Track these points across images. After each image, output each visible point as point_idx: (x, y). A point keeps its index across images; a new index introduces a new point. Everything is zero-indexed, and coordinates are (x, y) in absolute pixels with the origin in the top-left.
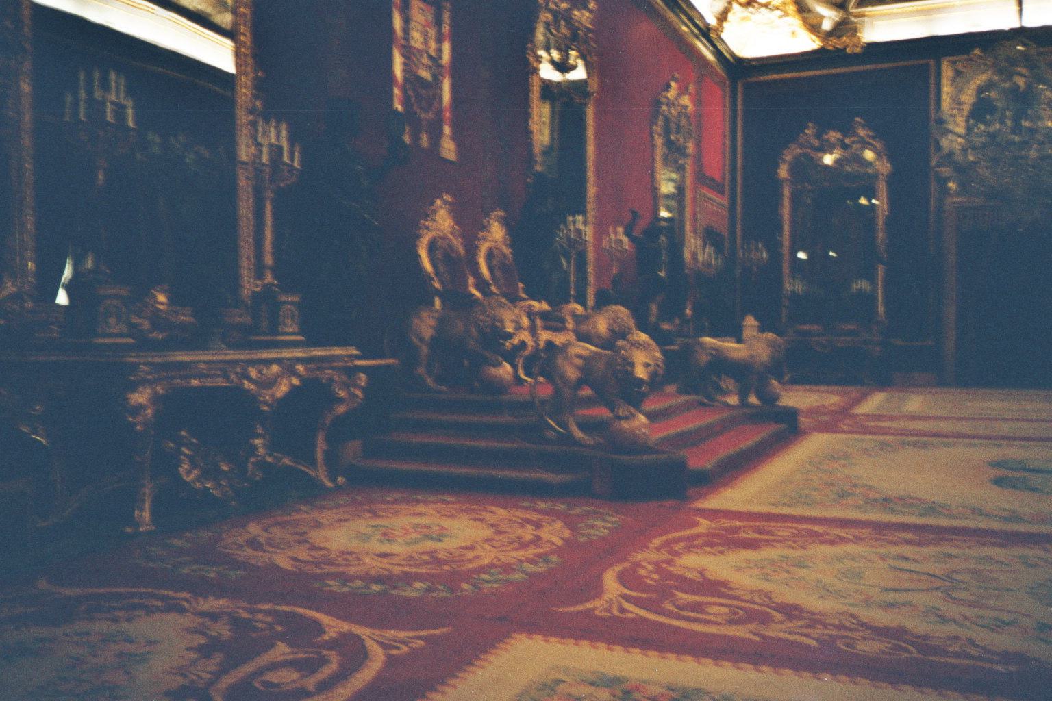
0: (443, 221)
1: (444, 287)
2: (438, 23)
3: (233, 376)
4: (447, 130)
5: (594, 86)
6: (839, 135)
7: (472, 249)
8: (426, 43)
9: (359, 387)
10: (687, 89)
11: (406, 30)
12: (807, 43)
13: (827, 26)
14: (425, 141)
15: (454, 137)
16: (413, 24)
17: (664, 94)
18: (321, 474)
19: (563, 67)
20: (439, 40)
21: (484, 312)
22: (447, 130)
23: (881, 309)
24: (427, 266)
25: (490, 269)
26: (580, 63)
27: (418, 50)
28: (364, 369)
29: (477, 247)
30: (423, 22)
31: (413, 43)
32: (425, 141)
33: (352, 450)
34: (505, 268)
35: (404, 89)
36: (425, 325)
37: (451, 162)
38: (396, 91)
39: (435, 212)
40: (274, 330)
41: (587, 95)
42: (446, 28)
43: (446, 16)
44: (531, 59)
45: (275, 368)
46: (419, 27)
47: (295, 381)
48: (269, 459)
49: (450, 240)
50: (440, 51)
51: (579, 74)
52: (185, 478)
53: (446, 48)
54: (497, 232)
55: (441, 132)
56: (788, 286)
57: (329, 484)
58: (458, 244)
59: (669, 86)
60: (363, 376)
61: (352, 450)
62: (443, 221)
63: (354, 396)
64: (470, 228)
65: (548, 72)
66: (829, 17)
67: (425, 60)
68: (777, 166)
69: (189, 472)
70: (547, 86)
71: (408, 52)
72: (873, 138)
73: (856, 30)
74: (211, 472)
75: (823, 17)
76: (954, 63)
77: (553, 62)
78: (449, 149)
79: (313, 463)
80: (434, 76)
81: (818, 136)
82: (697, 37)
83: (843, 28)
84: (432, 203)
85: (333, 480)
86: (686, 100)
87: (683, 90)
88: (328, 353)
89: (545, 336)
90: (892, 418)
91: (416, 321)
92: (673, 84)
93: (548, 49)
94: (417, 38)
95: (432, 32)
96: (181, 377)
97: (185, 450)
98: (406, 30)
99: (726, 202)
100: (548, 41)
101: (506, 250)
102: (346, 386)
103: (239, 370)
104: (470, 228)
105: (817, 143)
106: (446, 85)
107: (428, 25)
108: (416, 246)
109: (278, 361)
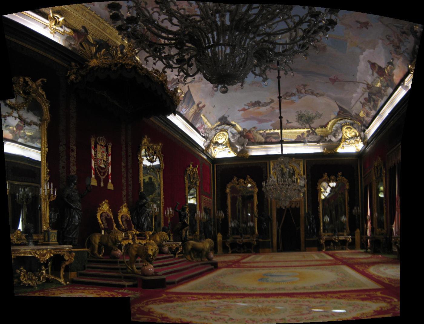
0: (105, 207)
1: (104, 227)
2: (107, 151)
3: (33, 253)
4: (110, 181)
5: (163, 166)
6: (243, 180)
7: (116, 216)
8: (103, 157)
9: (72, 257)
10: (196, 167)
11: (96, 154)
12: (232, 155)
13: (238, 150)
14: (102, 184)
15: (112, 182)
16: (98, 152)
17: (188, 168)
18: (62, 281)
19: (151, 161)
20: (107, 156)
21: (113, 235)
22: (110, 181)
23: (256, 231)
24: (100, 221)
25: (122, 222)
26: (158, 160)
27: (100, 159)
28: (75, 252)
29: (118, 215)
30: (102, 151)
31: (98, 157)
32: (102, 184)
33: (73, 275)
34: (127, 221)
35: (95, 170)
36: (97, 239)
37: (112, 190)
38: (93, 171)
39: (103, 205)
40: (49, 241)
41: (160, 169)
42: (110, 152)
43: (110, 149)
44: (140, 159)
45: (45, 252)
46: (100, 153)
47: (51, 255)
48: (47, 276)
49: (108, 213)
50: (107, 159)
51: (157, 163)
52: (22, 280)
53: (110, 158)
54: (124, 210)
55: (108, 181)
56: (230, 224)
57: (65, 284)
58: (111, 215)
59: (190, 166)
60: (74, 253)
61: (73, 275)
62: (105, 207)
63: (71, 259)
64: (115, 209)
65: (146, 163)
66: (239, 148)
67: (102, 162)
68: (226, 189)
69: (23, 279)
70: (145, 167)
71: (96, 160)
72: (253, 181)
73: (247, 152)
74: (31, 279)
75: (238, 148)
76: (274, 162)
77: (147, 159)
78: (110, 186)
79: (60, 277)
80: (105, 166)
81: (238, 180)
82: (200, 152)
83: (243, 151)
84: (102, 203)
85: (66, 282)
86: (195, 169)
87: (194, 166)
88: (61, 247)
89: (138, 241)
90: (254, 262)
91: (94, 237)
92: (191, 165)
93: (146, 157)
94: (99, 156)
95: (105, 154)
96: (18, 253)
97: (22, 273)
98: (96, 154)
99: (212, 200)
100: (146, 154)
101: (129, 216)
102: (69, 256)
103: (34, 252)
104: (115, 209)
105: (237, 182)
106: (110, 168)
107: (103, 152)
108: (96, 215)
109: (46, 249)
